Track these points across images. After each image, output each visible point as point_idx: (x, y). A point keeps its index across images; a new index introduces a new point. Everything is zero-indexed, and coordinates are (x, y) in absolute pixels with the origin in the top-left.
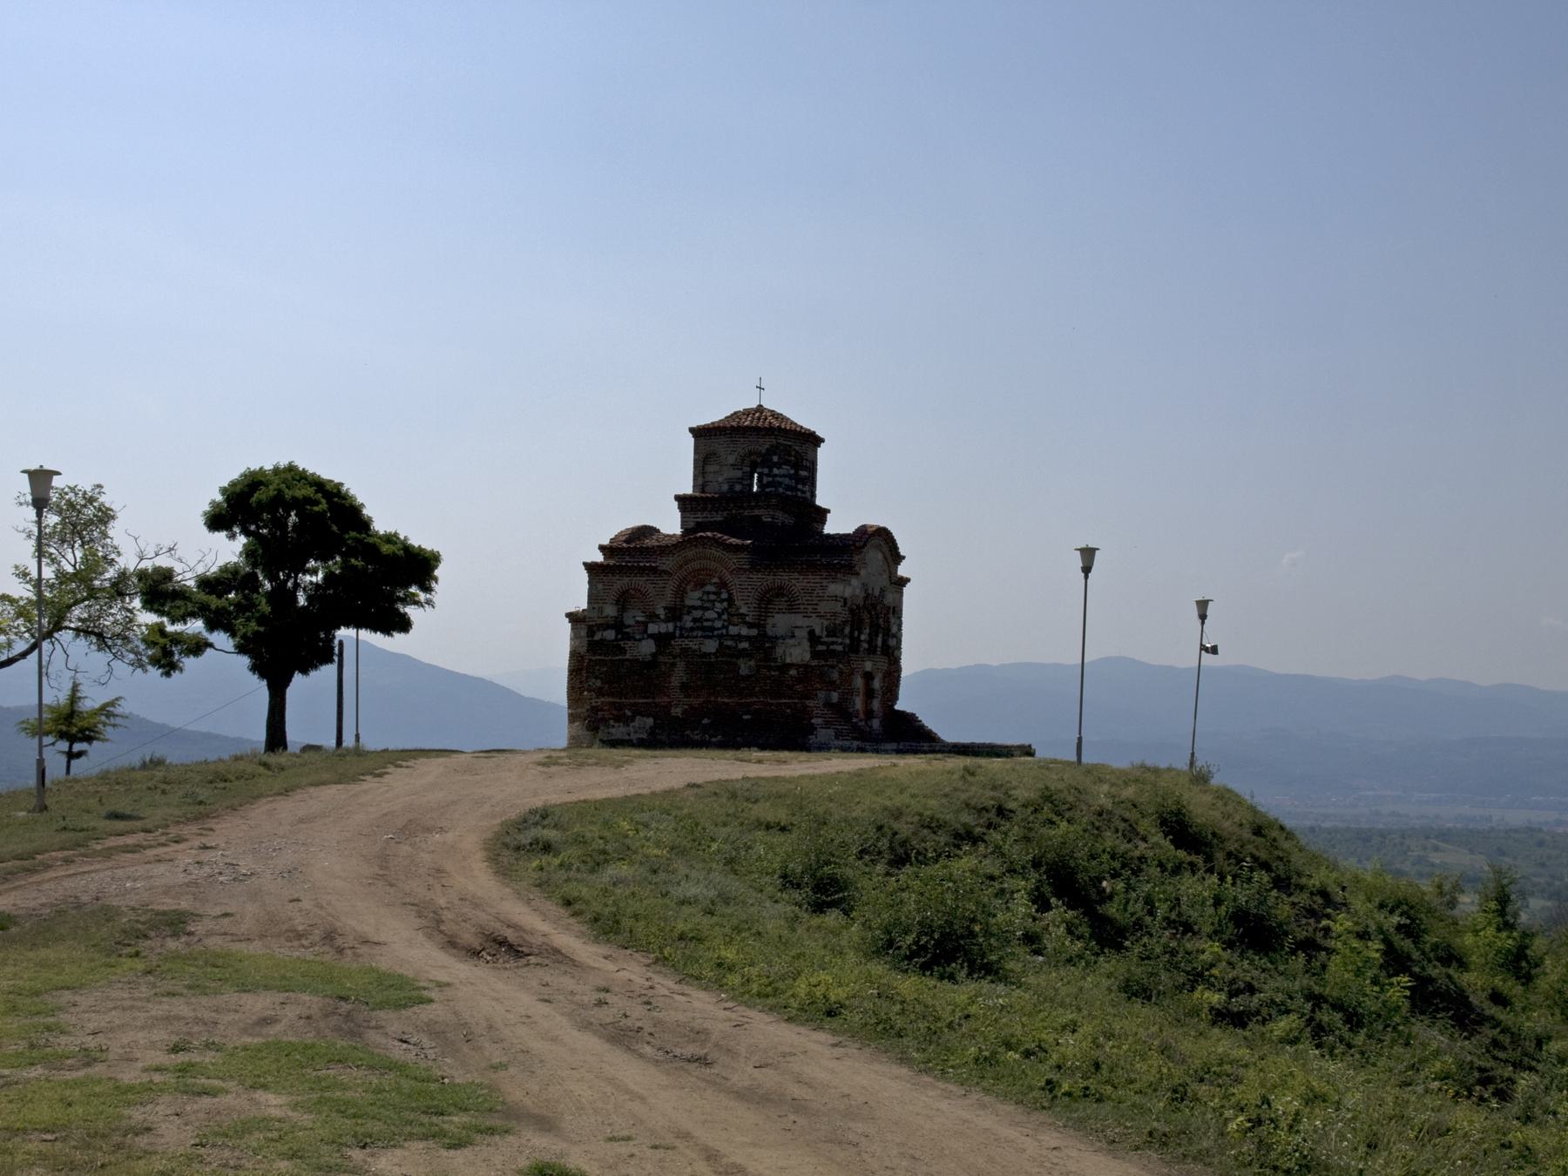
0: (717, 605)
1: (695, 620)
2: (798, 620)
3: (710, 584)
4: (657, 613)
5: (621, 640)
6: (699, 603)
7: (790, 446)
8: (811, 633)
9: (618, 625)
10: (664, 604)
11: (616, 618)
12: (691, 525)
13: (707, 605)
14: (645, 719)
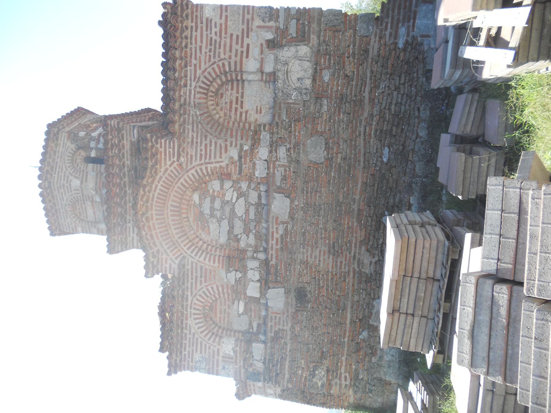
1: (247, 231)
2: (251, 65)
3: (200, 205)
4: (233, 282)
6: (225, 224)
7: (80, 124)
8: (272, 44)
10: (223, 273)
11: (237, 340)
13: (227, 209)
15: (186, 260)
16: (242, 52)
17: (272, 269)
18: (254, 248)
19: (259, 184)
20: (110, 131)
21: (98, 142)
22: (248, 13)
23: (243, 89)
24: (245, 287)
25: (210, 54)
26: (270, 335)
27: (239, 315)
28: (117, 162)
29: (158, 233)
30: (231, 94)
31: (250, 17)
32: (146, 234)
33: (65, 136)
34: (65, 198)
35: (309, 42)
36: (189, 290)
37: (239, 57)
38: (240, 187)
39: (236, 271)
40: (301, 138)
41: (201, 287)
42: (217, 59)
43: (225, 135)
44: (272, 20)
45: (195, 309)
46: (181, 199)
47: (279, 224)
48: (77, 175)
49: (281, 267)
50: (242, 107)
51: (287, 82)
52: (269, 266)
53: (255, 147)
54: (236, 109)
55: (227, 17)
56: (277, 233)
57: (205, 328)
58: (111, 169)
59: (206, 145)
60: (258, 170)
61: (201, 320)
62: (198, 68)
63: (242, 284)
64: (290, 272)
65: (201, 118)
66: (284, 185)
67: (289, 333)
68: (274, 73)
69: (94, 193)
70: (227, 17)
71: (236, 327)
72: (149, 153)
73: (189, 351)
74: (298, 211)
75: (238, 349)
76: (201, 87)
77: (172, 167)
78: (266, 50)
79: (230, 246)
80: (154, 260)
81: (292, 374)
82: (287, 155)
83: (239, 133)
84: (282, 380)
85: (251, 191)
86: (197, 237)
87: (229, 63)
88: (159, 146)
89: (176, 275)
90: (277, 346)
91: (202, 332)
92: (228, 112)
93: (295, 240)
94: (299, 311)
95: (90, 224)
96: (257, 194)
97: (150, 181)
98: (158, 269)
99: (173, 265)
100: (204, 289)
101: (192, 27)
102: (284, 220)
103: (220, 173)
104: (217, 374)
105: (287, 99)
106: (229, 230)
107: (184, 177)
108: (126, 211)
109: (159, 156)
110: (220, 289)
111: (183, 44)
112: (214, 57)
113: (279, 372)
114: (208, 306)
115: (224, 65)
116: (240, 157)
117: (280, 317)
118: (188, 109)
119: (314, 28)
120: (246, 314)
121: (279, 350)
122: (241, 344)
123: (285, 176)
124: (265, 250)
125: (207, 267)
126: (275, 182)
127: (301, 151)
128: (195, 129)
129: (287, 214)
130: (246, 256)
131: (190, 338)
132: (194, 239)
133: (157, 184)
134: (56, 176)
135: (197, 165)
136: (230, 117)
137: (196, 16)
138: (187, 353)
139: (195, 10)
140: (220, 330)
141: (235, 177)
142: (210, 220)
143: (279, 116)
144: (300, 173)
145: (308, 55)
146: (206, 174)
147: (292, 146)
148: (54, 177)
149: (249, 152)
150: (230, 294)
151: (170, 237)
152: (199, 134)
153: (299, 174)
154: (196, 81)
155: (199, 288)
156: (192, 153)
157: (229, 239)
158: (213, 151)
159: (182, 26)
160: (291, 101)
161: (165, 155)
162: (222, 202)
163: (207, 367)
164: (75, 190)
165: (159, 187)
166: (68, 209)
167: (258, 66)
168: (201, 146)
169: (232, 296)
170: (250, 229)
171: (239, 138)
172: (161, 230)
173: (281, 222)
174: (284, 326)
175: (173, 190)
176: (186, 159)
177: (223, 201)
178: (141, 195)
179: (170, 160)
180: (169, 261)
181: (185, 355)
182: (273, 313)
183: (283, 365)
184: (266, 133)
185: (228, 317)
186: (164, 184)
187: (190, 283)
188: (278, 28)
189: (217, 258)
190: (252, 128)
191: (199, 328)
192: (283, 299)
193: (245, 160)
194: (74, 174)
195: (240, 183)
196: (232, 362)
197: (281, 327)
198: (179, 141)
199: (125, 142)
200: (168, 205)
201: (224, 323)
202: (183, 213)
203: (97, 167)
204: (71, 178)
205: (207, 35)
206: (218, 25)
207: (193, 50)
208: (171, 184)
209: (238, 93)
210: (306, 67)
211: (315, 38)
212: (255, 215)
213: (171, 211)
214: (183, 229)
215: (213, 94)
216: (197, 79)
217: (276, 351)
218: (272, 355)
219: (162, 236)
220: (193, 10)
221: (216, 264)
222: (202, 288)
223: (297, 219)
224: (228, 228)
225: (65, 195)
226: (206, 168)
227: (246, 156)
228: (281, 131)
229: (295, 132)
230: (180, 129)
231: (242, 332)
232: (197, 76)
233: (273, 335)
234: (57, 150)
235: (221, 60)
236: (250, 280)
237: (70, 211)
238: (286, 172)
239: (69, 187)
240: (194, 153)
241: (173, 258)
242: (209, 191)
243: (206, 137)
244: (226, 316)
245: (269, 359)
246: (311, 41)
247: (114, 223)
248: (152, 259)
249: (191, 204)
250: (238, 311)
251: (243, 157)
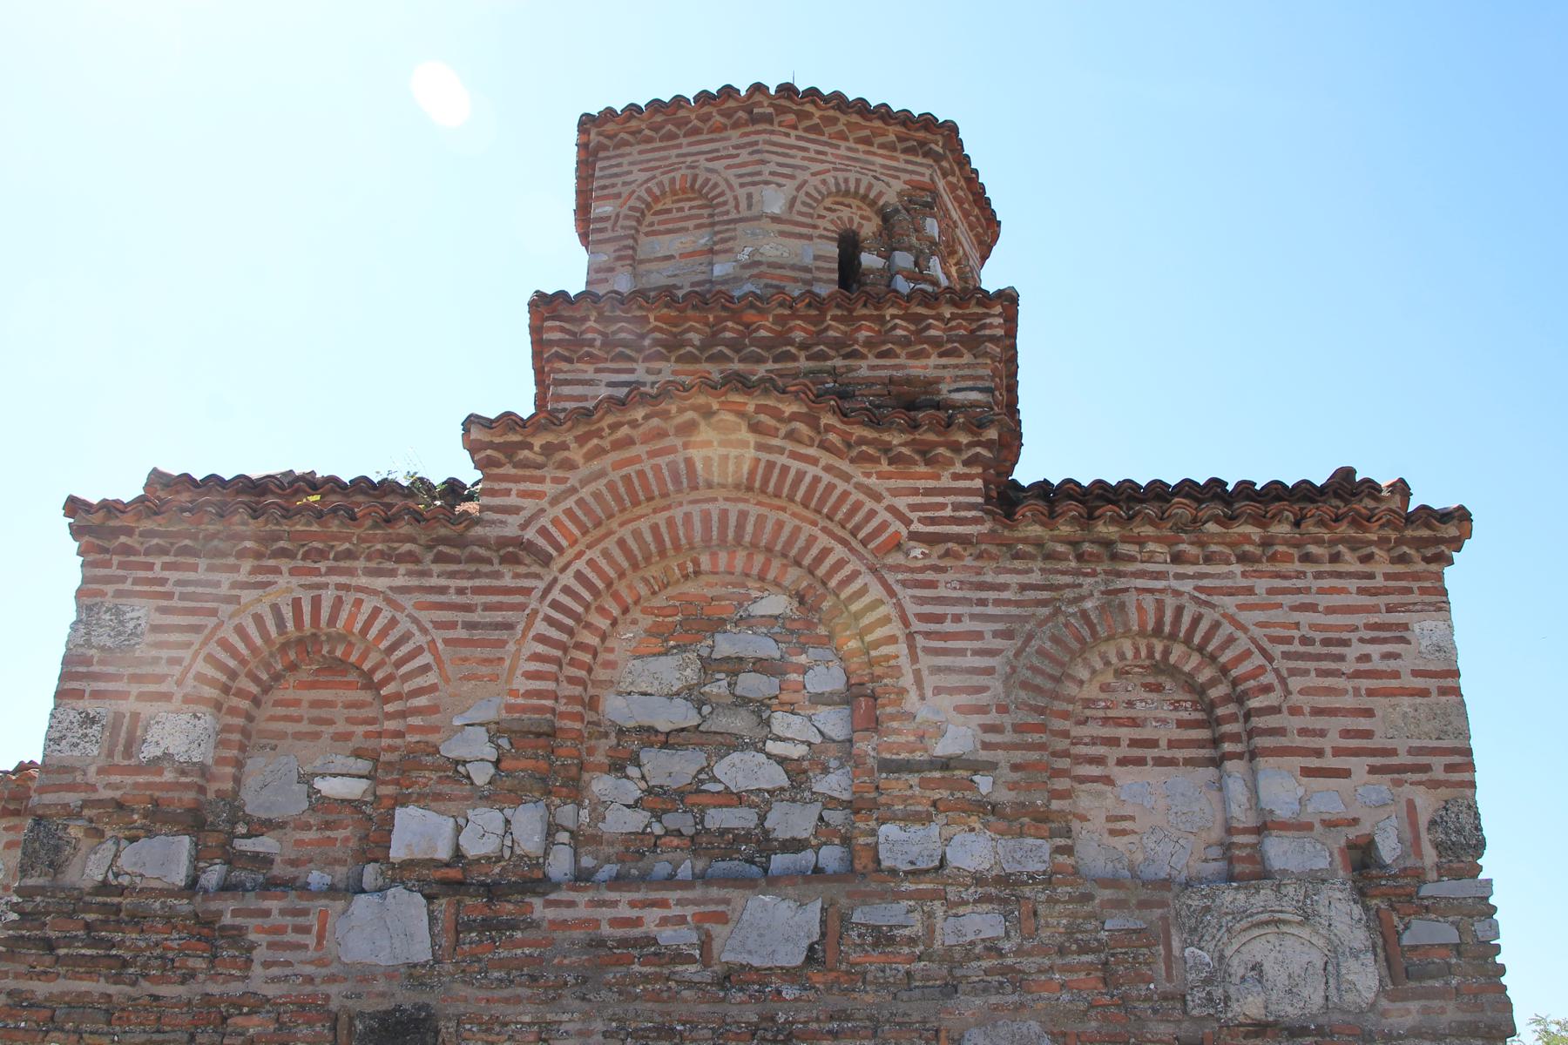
1: (657, 800)
4: (452, 750)
5: (226, 887)
6: (681, 715)
8: (1362, 858)
10: (489, 712)
11: (203, 769)
13: (739, 723)
15: (536, 569)
16: (1319, 753)
17: (510, 907)
18: (590, 831)
19: (846, 841)
20: (967, 311)
22: (1449, 768)
23: (1189, 762)
24: (427, 799)
25: (1296, 642)
26: (227, 910)
27: (306, 779)
28: (864, 334)
29: (638, 467)
30: (1164, 721)
31: (1439, 774)
32: (634, 424)
33: (923, 175)
35: (1393, 998)
36: (414, 582)
37: (1300, 741)
38: (826, 770)
39: (497, 764)
40: (1045, 995)
41: (429, 626)
42: (1284, 665)
43: (1025, 704)
44: (1440, 856)
45: (339, 602)
46: (769, 549)
47: (698, 928)
48: (798, 206)
49: (521, 944)
50: (1122, 762)
51: (1244, 923)
52: (523, 893)
53: (991, 818)
54: (1114, 742)
55: (1424, 693)
56: (664, 921)
57: (259, 642)
58: (839, 312)
59: (979, 635)
60: (903, 835)
61: (290, 625)
62: (1241, 599)
63: (446, 788)
64: (501, 980)
65: (1073, 615)
66: (858, 941)
67: (236, 988)
68: (1265, 874)
69: (744, 257)
70: (1424, 693)
71: (256, 765)
72: (931, 437)
73: (162, 582)
74: (758, 1000)
75: (169, 776)
76: (1179, 610)
77: (888, 516)
79: (591, 736)
80: (537, 449)
81: (47, 1013)
82: (972, 943)
83: (1034, 756)
84: (23, 968)
85: (815, 809)
86: (626, 611)
87: (1275, 710)
88: (959, 468)
89: (478, 531)
90: (175, 940)
91: (241, 631)
92: (1101, 714)
93: (637, 997)
94: (334, 1028)
95: (630, 242)
96: (804, 835)
97: (832, 437)
98: (499, 465)
99: (514, 521)
100: (419, 639)
101: (1371, 576)
102: (716, 945)
103: (879, 690)
104: (60, 694)
105: (1181, 928)
106: (657, 731)
107: (853, 558)
108: (693, 359)
109: (922, 469)
110: (422, 701)
111: (1313, 549)
112: (1286, 655)
113: (62, 952)
114: (347, 653)
115: (1267, 689)
116: (946, 764)
117: (306, 947)
118: (1099, 569)
119: (1443, 1011)
120: (312, 808)
121: (158, 951)
122: (186, 786)
123: (891, 940)
124: (582, 878)
125: (511, 647)
126: (865, 903)
127: (994, 999)
128: (1030, 595)
129: (744, 959)
130: (557, 801)
131: (218, 584)
132: (616, 596)
133: (823, 463)
134: (792, 141)
135: (899, 606)
136: (1084, 722)
137: (1409, 591)
138: (158, 572)
139: (1427, 584)
140: (245, 704)
142: (693, 656)
143: (1119, 904)
144: (910, 1000)
145: (1349, 997)
146: (868, 638)
147: (1009, 961)
148: (787, 135)
149: (969, 795)
150: (399, 741)
151: (623, 510)
152: (1014, 611)
153: (904, 995)
154: (1197, 594)
155: (424, 616)
156: (942, 585)
157: (621, 732)
158: (959, 661)
159: (1370, 543)
160: (1176, 944)
161: (929, 492)
163: (93, 652)
164: (750, 196)
165: (812, 471)
166: (678, 175)
167: (1283, 813)
168: (973, 617)
169: (392, 749)
170: (665, 812)
171: (1018, 756)
172: (650, 475)
173: (708, 935)
174: (267, 965)
175: (804, 519)
176: (920, 564)
177: (769, 707)
178: (780, 406)
179: (913, 508)
180: (530, 505)
181: (150, 567)
182: (323, 916)
183: (90, 967)
184: (1046, 858)
185: (298, 736)
186: (821, 487)
187: (443, 582)
188: (1418, 875)
189: (549, 685)
190: (1056, 805)
191: (258, 619)
192: (384, 959)
193: (939, 784)
194: (802, 196)
195: (842, 766)
196: (110, 754)
197: (259, 954)
198: (982, 538)
199: (934, 360)
200: (746, 501)
201: (273, 718)
202: (714, 555)
203: (830, 270)
204: (790, 186)
205: (1356, 629)
206: (1392, 664)
207: (1300, 583)
208: (825, 510)
209: (1172, 744)
210: (1305, 993)
211: (1410, 1021)
212: (723, 832)
213: (724, 514)
214: (671, 553)
215: (1158, 656)
216: (1203, 597)
217: (154, 938)
218: (138, 920)
219: (627, 479)
220: (1426, 579)
221: (522, 684)
222: (424, 631)
223: (723, 1000)
224: (663, 726)
225: (728, 167)
226: (892, 640)
227: (953, 785)
228: (1061, 915)
229: (1065, 969)
230: (1025, 541)
231: (236, 793)
232: (1215, 599)
233: (227, 919)
234: (874, 149)
235: (1283, 681)
236: (461, 821)
237: (673, 181)
238: (908, 945)
239: (757, 179)
240: (942, 591)
241: (544, 521)
242: (803, 651)
243: (1008, 635)
244: (304, 727)
245: (117, 909)
246: (1399, 1005)
247: (645, 319)
248: (537, 443)
249: (750, 584)
250: (323, 776)
251: (947, 774)
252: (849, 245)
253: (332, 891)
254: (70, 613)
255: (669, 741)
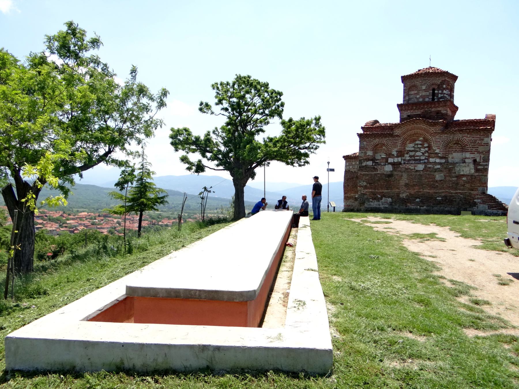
0: (422, 149)
1: (410, 156)
2: (468, 155)
3: (419, 140)
4: (393, 153)
5: (375, 165)
6: (413, 149)
8: (475, 161)
9: (373, 160)
10: (396, 150)
12: (405, 116)
13: (418, 149)
14: (387, 199)
21: (441, 94)
31: (484, 153)
34: (418, 82)
69: (420, 95)
78: (473, 159)
116: (436, 153)
124: (404, 163)
141: (429, 152)
162: (421, 148)
180: (398, 132)
183: (365, 172)
204: (426, 85)
252: (434, 90)
253: (384, 165)
254: (359, 143)
255: (412, 151)
